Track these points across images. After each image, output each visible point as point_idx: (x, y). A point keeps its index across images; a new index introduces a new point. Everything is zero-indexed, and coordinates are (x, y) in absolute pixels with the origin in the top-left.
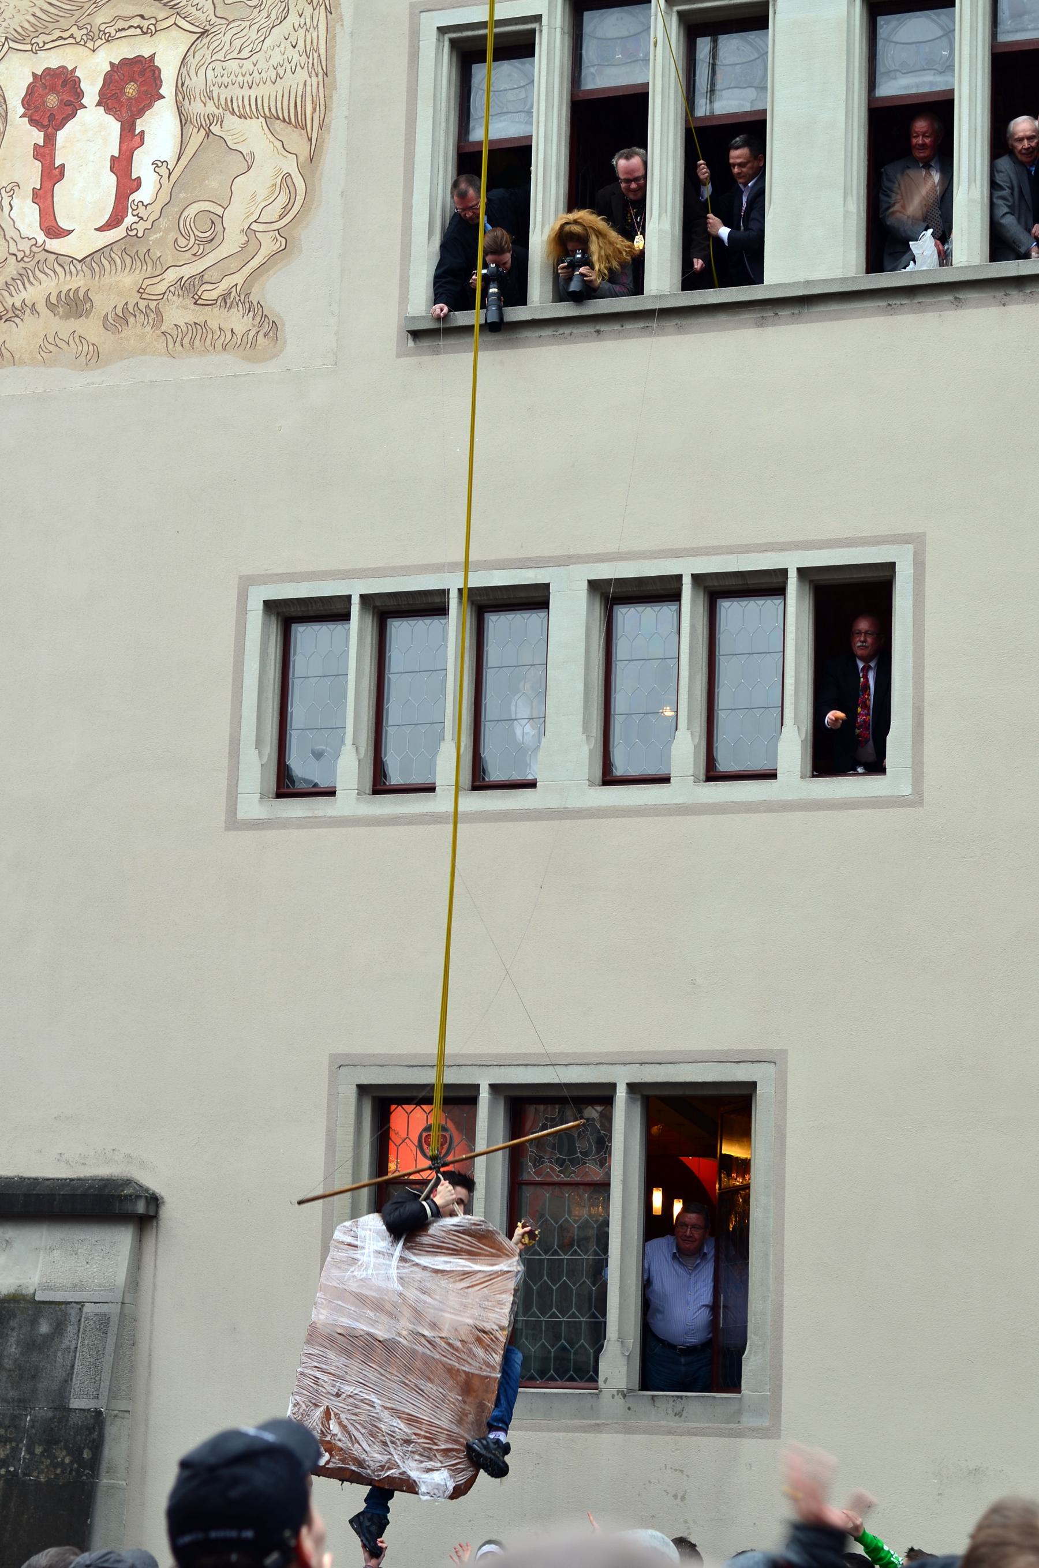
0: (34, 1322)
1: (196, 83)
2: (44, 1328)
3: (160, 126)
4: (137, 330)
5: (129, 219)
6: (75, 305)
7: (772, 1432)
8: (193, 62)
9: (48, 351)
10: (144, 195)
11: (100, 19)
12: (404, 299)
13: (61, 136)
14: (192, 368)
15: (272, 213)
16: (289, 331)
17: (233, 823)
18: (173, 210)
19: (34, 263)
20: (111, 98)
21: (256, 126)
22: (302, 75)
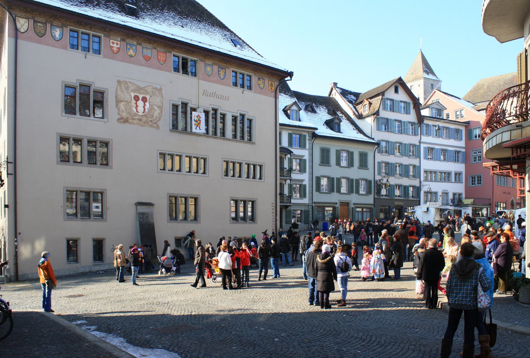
3: (147, 104)
4: (146, 124)
6: (140, 120)
10: (146, 111)
19: (136, 115)
20: (142, 100)
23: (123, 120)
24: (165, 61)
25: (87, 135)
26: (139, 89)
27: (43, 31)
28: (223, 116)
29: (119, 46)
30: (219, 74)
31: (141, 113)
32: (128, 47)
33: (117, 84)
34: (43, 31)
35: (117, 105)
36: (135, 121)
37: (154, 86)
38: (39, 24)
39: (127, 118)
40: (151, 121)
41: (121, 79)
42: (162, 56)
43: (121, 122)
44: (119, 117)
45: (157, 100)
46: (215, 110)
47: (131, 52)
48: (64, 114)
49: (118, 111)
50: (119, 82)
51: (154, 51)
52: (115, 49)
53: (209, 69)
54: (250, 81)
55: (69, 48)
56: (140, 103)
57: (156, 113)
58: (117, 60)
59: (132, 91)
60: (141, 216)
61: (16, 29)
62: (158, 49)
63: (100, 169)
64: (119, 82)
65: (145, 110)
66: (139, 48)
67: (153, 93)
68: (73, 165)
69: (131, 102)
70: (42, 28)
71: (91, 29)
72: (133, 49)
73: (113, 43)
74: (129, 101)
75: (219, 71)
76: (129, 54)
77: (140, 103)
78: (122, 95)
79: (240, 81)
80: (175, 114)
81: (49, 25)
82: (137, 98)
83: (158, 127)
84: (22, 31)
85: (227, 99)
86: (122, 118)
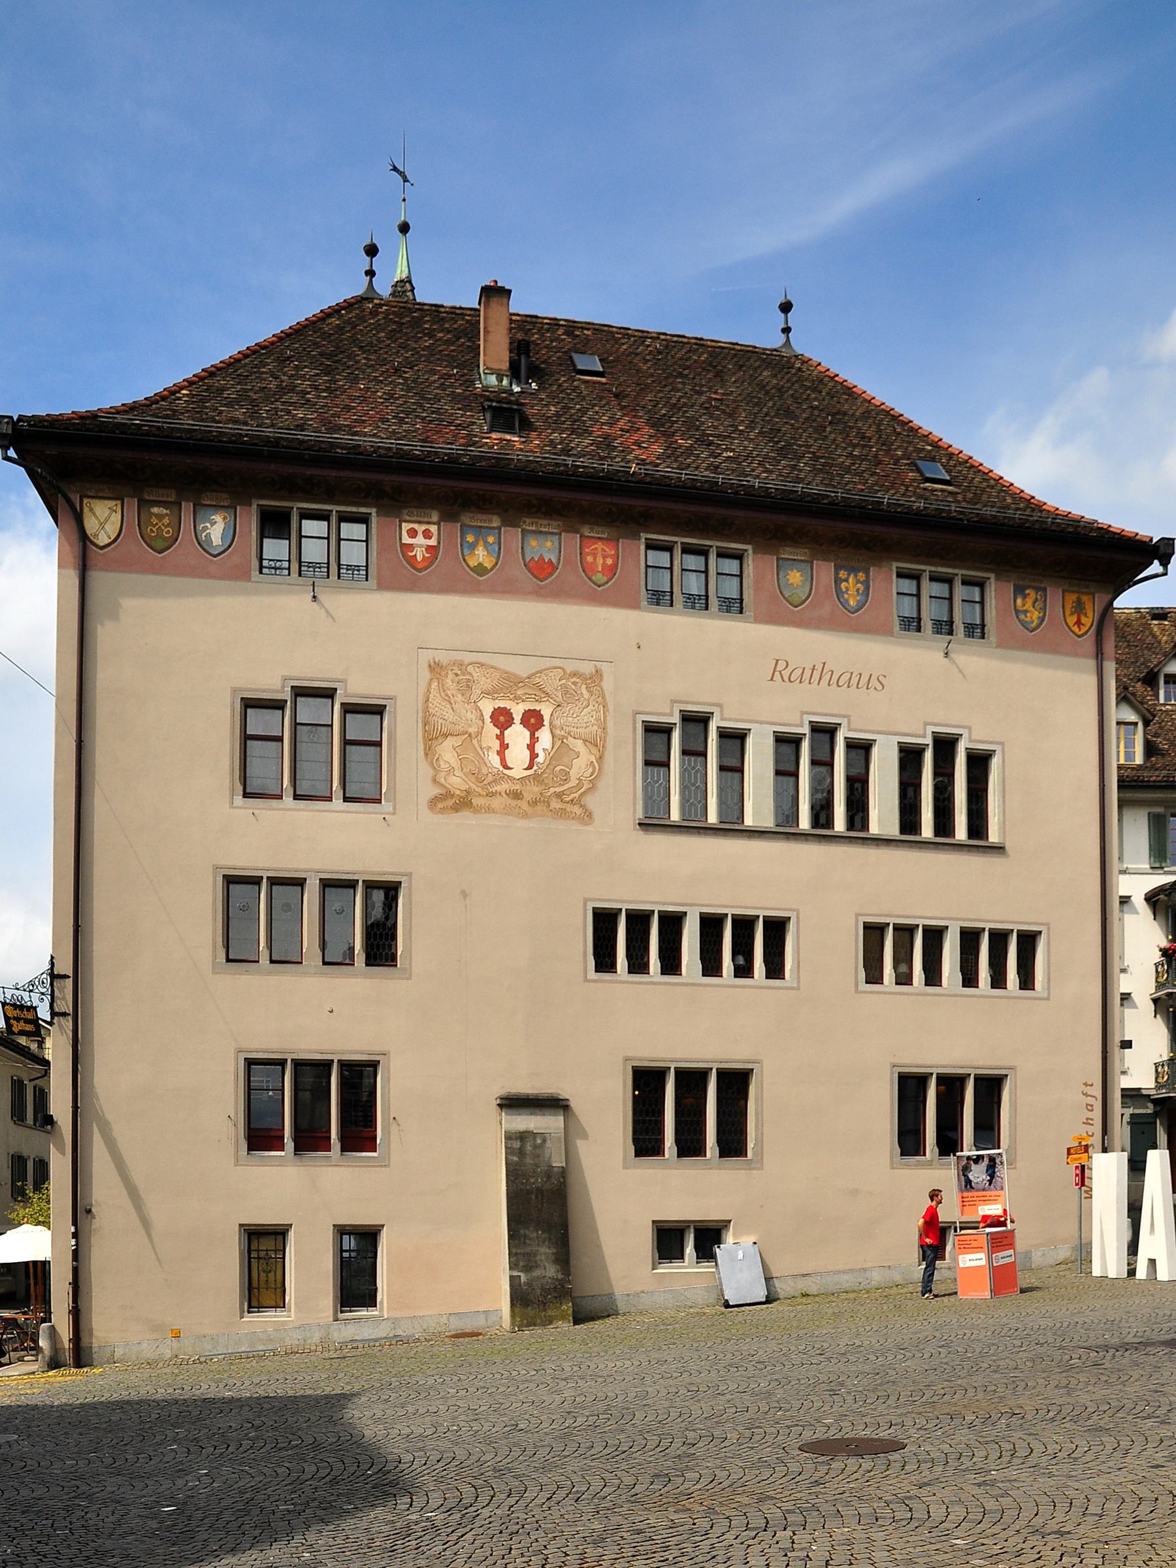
0: (535, 1139)
1: (557, 722)
2: (539, 1141)
3: (544, 735)
4: (539, 807)
5: (535, 768)
6: (517, 795)
7: (761, 1168)
8: (556, 715)
9: (507, 811)
10: (540, 759)
11: (519, 692)
12: (634, 812)
13: (506, 732)
14: (562, 825)
15: (588, 774)
16: (595, 815)
17: (586, 980)
18: (551, 767)
19: (499, 778)
20: (525, 722)
21: (580, 742)
22: (595, 728)
23: (450, 803)
24: (612, 570)
25: (317, 866)
26: (510, 684)
27: (168, 532)
28: (860, 749)
29: (433, 542)
30: (839, 593)
31: (518, 772)
32: (470, 538)
33: (426, 674)
34: (168, 532)
35: (429, 751)
36: (496, 803)
37: (570, 666)
38: (155, 510)
39: (468, 792)
40: (559, 796)
41: (443, 657)
42: (600, 553)
43: (443, 811)
44: (437, 791)
45: (582, 718)
46: (824, 732)
47: (481, 556)
48: (239, 799)
49: (431, 772)
50: (435, 668)
51: (572, 541)
52: (420, 554)
53: (795, 577)
54: (982, 603)
55: (255, 573)
56: (517, 735)
57: (581, 763)
58: (429, 590)
59: (490, 694)
60: (517, 1145)
61: (84, 539)
62: (586, 531)
63: (368, 982)
64: (435, 668)
65: (534, 756)
66: (512, 536)
67: (566, 691)
68: (270, 973)
69: (479, 733)
70: (166, 521)
71: (330, 498)
72: (486, 543)
73: (413, 533)
74: (470, 730)
75: (838, 581)
76: (473, 563)
77: (517, 735)
78: (448, 714)
79: (930, 611)
80: (656, 762)
81: (187, 508)
82: (502, 719)
83: (589, 814)
84: (103, 540)
85: (873, 682)
86: (448, 795)
